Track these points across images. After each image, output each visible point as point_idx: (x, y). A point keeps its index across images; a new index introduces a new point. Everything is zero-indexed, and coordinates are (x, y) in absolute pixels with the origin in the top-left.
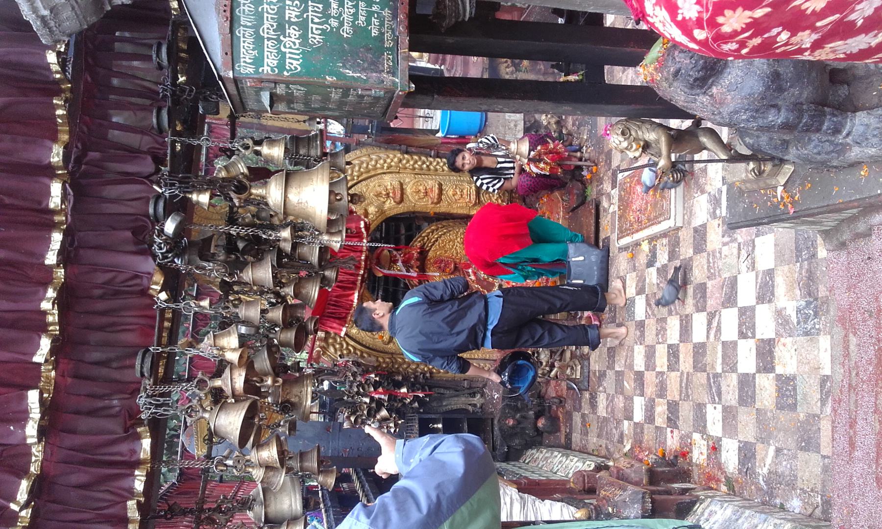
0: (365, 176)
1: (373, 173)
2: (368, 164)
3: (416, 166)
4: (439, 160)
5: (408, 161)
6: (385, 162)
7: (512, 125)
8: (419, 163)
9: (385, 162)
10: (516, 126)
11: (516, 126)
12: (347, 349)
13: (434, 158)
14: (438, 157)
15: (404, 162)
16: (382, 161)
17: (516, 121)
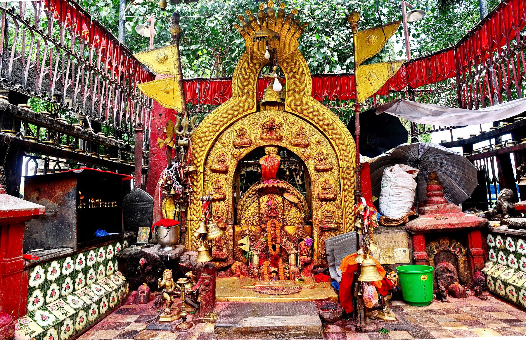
0: (333, 143)
1: (336, 148)
2: (343, 144)
3: (346, 180)
4: (353, 198)
5: (349, 174)
6: (346, 156)
7: (390, 254)
8: (349, 183)
9: (346, 156)
10: (390, 257)
11: (390, 257)
13: (354, 194)
14: (355, 196)
15: (348, 171)
16: (346, 154)
17: (393, 257)
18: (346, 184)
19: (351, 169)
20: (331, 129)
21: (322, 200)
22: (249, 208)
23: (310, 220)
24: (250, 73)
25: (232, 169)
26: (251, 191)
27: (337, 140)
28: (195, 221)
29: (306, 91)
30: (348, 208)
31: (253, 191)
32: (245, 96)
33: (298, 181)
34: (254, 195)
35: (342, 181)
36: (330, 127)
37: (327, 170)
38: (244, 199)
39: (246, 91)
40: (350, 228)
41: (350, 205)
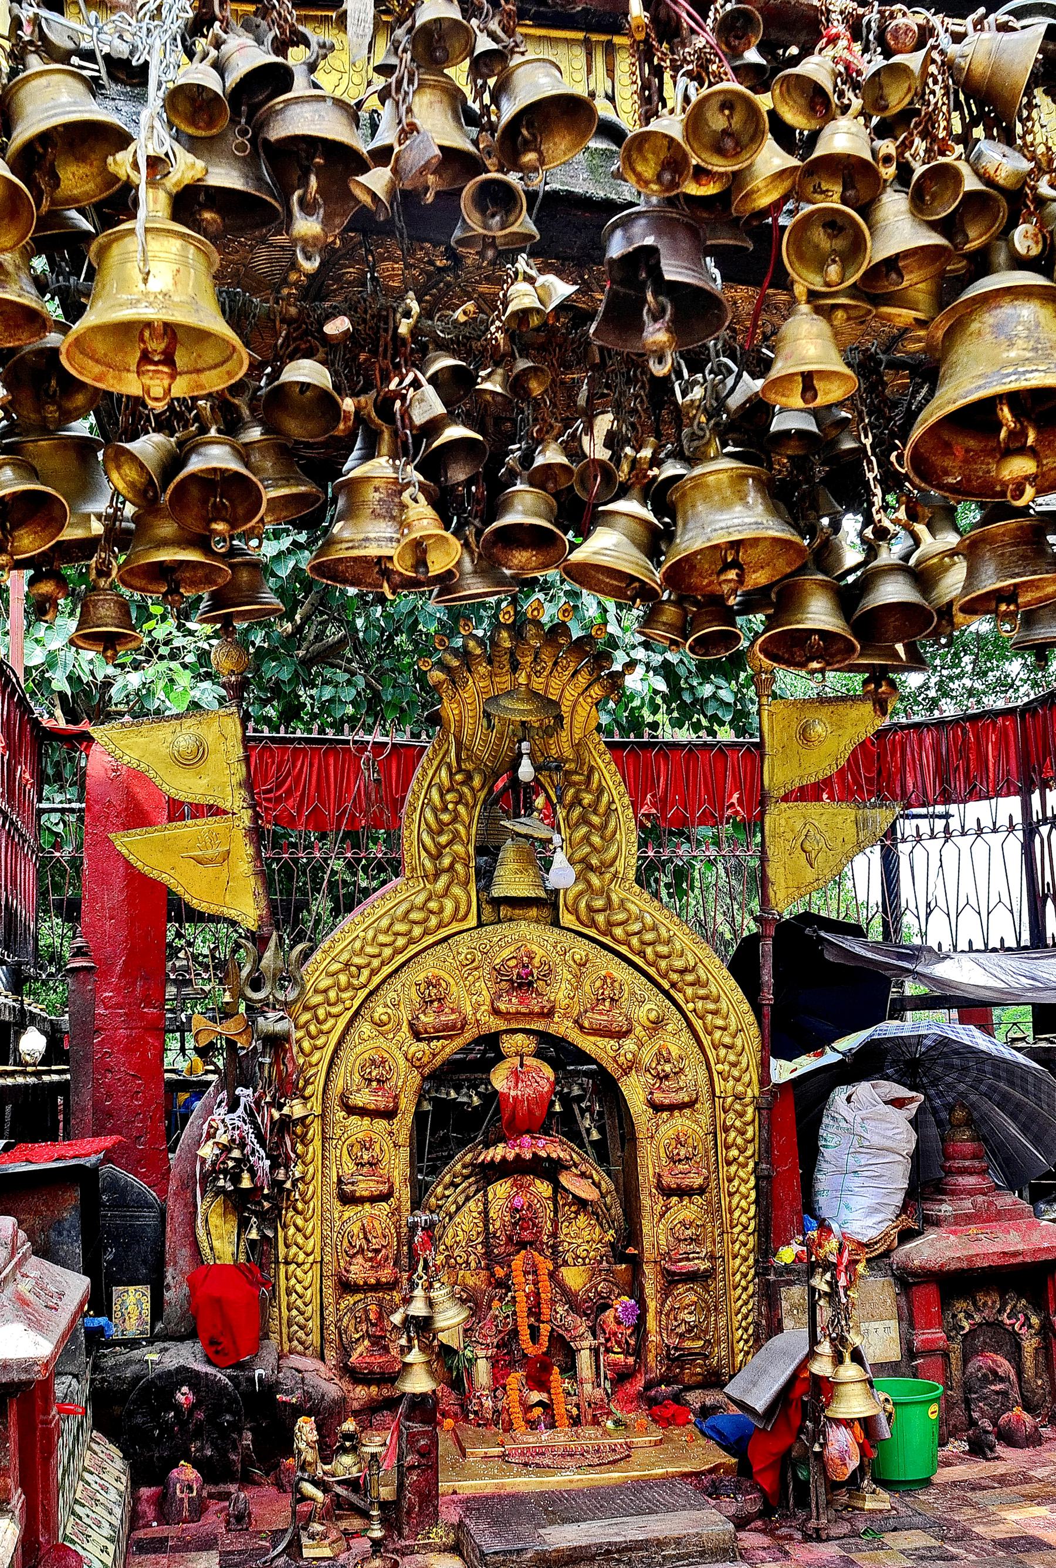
0: (698, 1024)
1: (706, 1041)
2: (724, 1029)
3: (733, 1134)
4: (752, 1183)
6: (734, 1065)
8: (739, 1141)
9: (734, 1065)
12: (329, 1015)
13: (754, 1171)
14: (757, 1178)
16: (732, 1058)
18: (734, 1144)
19: (747, 1100)
20: (692, 984)
21: (667, 1192)
22: (457, 1219)
23: (631, 1250)
24: (457, 803)
25: (407, 1104)
26: (459, 1166)
27: (710, 1017)
28: (299, 1265)
29: (619, 865)
30: (737, 1214)
31: (464, 1167)
32: (444, 879)
33: (588, 1131)
34: (467, 1177)
35: (721, 1136)
36: (690, 978)
37: (681, 1106)
38: (439, 1189)
39: (446, 862)
40: (743, 1269)
41: (743, 1204)
